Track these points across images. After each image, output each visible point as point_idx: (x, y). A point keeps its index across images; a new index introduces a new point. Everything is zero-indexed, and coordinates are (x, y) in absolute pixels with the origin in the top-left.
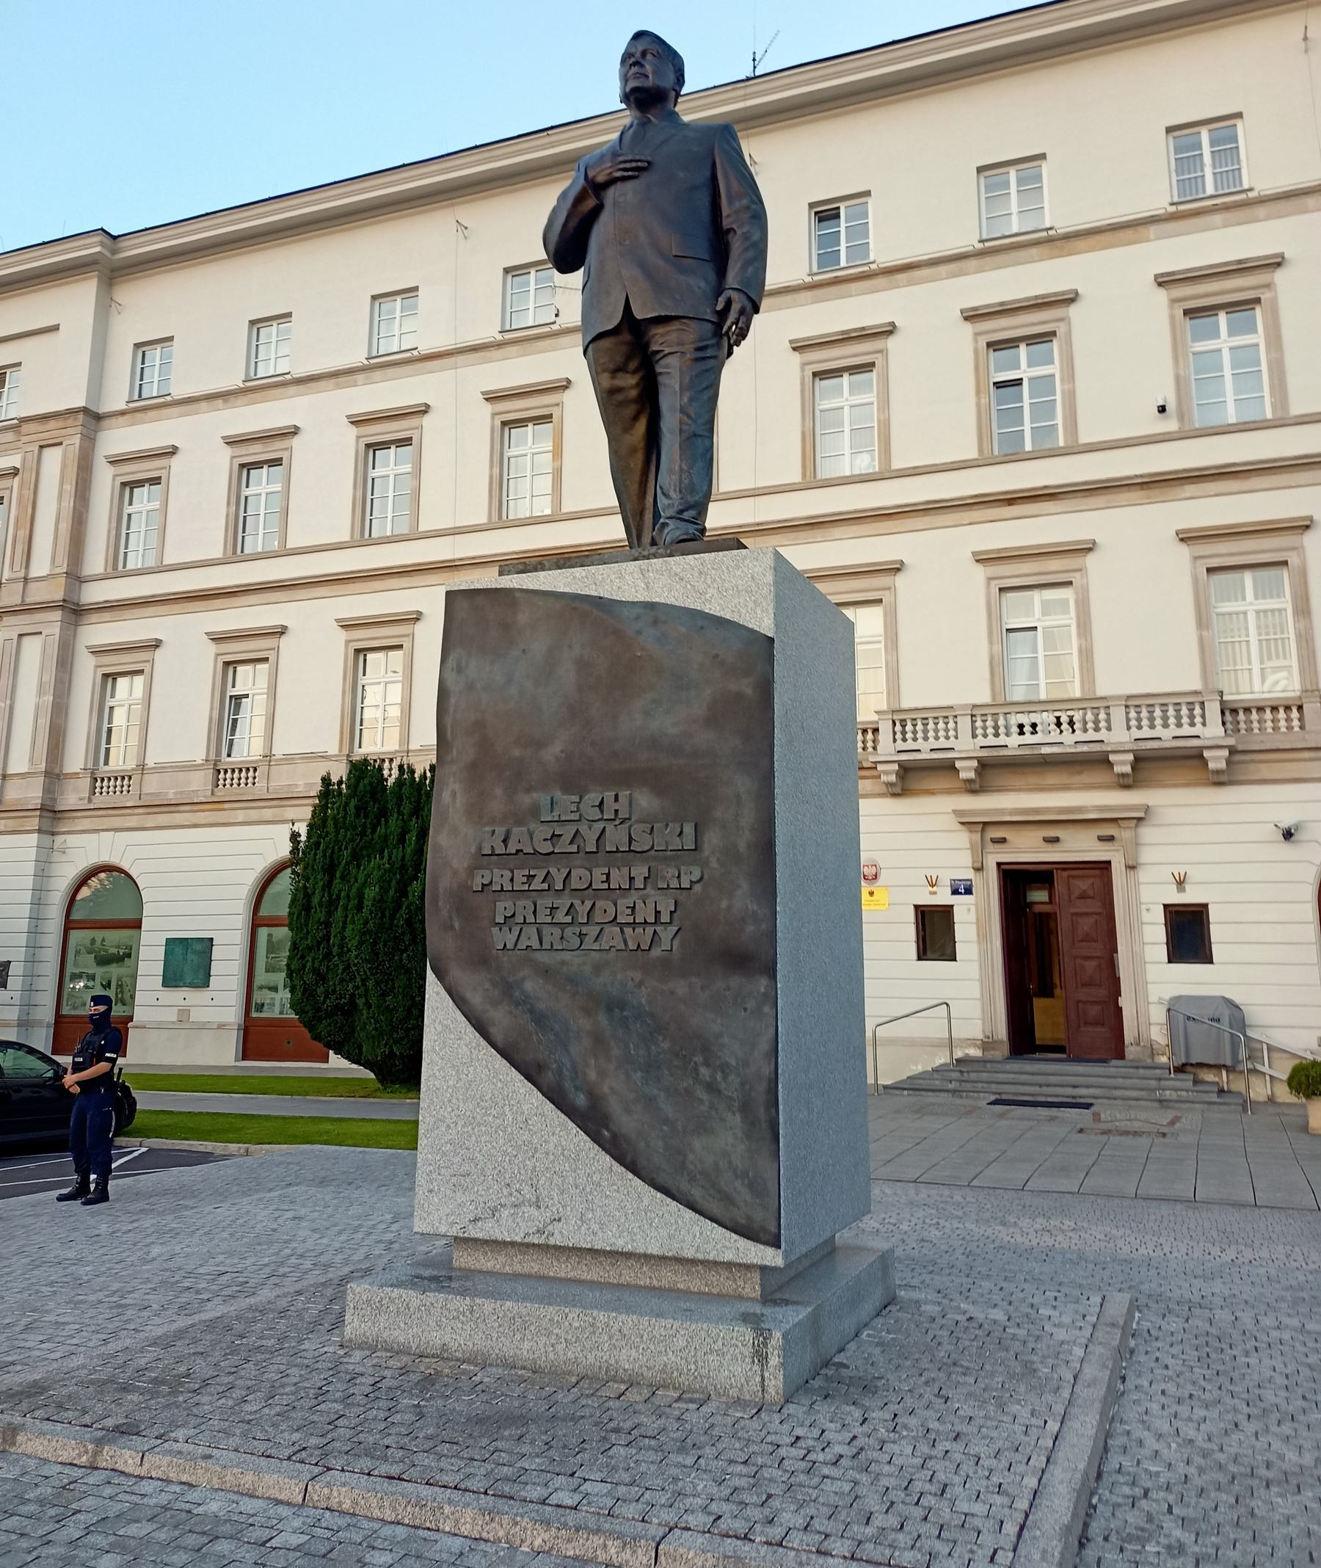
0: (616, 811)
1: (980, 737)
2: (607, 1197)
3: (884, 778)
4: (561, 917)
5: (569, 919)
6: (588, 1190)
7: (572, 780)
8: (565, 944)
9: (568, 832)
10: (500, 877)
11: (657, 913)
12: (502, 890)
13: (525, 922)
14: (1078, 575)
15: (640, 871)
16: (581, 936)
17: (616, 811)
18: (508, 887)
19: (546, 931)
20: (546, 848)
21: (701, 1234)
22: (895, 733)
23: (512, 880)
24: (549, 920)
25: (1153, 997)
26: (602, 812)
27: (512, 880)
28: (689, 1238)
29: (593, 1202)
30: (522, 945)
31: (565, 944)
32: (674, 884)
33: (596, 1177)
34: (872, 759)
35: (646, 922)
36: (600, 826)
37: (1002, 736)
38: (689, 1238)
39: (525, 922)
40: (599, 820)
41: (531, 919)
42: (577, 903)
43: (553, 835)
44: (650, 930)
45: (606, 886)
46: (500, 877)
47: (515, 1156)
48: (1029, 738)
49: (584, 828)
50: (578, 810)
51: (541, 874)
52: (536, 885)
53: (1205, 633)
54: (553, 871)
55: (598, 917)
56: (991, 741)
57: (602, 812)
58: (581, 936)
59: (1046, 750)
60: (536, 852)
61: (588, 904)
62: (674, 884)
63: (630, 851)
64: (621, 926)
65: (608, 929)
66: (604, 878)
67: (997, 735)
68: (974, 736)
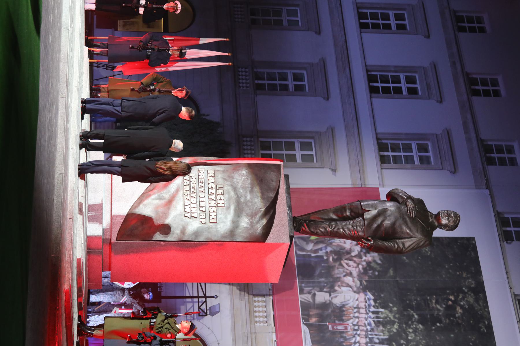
0: (219, 203)
4: (192, 190)
8: (185, 191)
11: (194, 213)
12: (199, 176)
13: (191, 181)
16: (187, 195)
17: (219, 203)
18: (200, 177)
19: (188, 187)
21: (118, 224)
24: (191, 187)
27: (201, 178)
30: (185, 181)
31: (185, 191)
35: (191, 210)
39: (191, 181)
40: (217, 199)
41: (191, 183)
43: (213, 188)
44: (189, 211)
45: (200, 201)
50: (219, 194)
51: (203, 185)
58: (187, 195)
60: (209, 184)
61: (195, 197)
62: (201, 217)
63: (209, 207)
66: (202, 200)
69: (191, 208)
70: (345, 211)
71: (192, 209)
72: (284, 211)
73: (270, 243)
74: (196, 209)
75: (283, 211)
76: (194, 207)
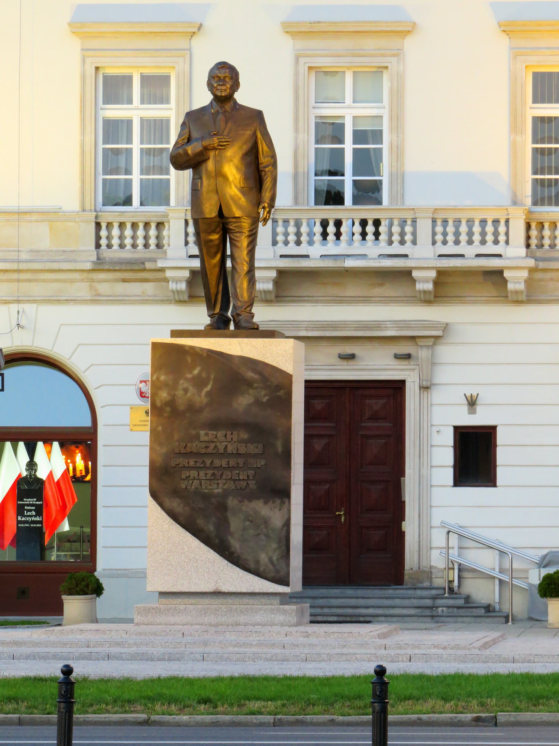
0: (232, 439)
1: (280, 245)
2: (226, 574)
3: (172, 286)
5: (213, 478)
6: (219, 572)
7: (214, 425)
9: (212, 446)
10: (182, 461)
11: (248, 476)
14: (394, 60)
15: (241, 461)
17: (232, 439)
19: (203, 482)
20: (203, 451)
21: (261, 584)
22: (187, 234)
23: (188, 463)
24: (204, 478)
25: (436, 522)
26: (226, 438)
28: (257, 586)
29: (220, 576)
32: (255, 466)
33: (221, 568)
34: (160, 264)
36: (226, 443)
37: (304, 245)
38: (257, 586)
41: (197, 477)
42: (216, 472)
45: (227, 466)
46: (182, 461)
47: (189, 563)
48: (331, 247)
49: (218, 444)
52: (198, 465)
53: (519, 138)
54: (206, 460)
55: (224, 477)
56: (292, 249)
57: (226, 438)
59: (350, 263)
61: (221, 472)
64: (234, 480)
65: (229, 482)
67: (298, 243)
68: (275, 243)
69: (240, 480)
70: (211, 241)
71: (241, 478)
72: (239, 343)
73: (293, 367)
74: (241, 473)
75: (240, 345)
76: (237, 475)
